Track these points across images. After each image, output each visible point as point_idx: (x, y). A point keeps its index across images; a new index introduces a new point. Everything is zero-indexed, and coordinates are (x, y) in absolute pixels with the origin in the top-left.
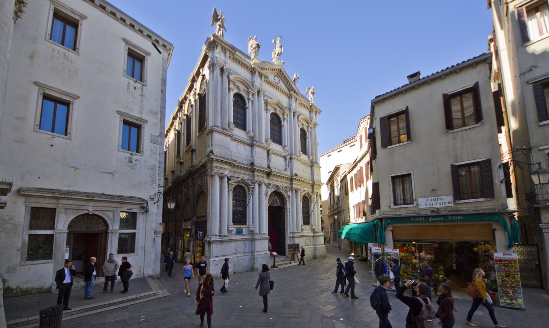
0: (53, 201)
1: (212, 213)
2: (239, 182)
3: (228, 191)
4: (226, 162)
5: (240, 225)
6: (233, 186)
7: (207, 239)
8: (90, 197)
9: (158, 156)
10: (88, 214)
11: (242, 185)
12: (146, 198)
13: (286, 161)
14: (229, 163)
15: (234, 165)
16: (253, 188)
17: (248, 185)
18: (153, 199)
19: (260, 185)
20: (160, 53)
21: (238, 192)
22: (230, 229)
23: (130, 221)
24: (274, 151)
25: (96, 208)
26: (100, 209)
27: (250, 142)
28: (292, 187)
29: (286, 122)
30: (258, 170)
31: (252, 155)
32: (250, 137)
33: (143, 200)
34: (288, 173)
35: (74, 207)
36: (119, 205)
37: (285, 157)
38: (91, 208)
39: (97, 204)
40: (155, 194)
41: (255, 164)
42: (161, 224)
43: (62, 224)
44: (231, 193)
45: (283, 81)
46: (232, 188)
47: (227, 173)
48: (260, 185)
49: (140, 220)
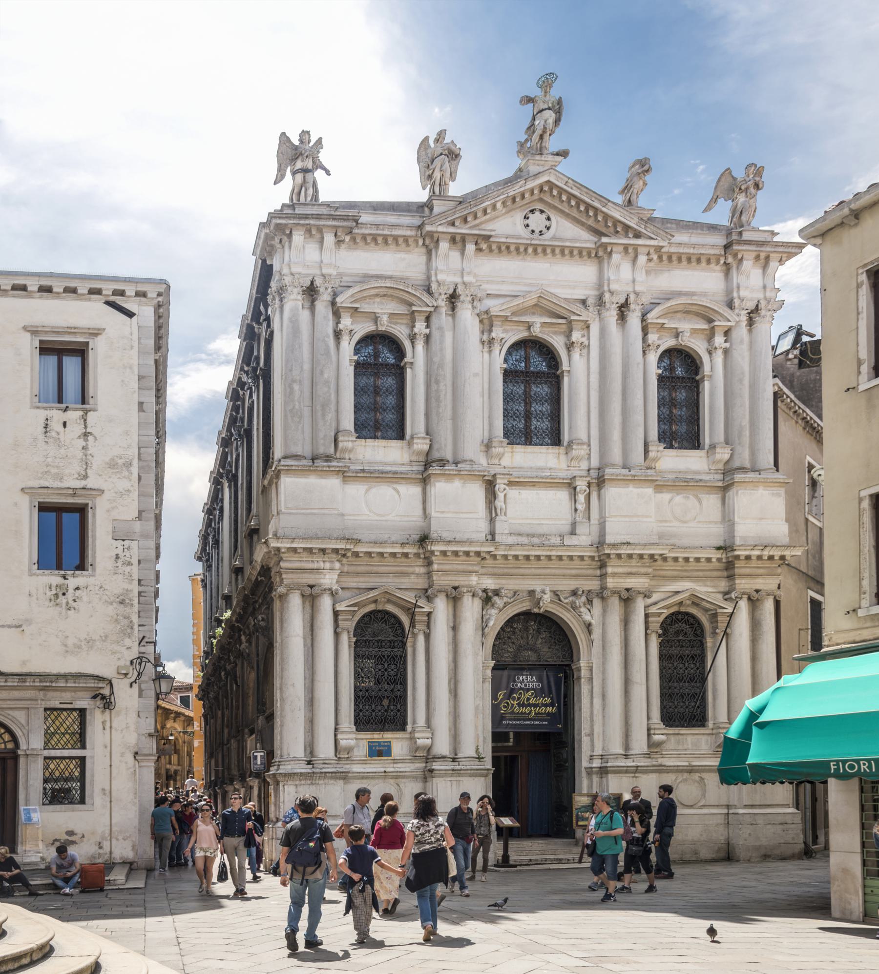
1: (282, 699)
2: (376, 601)
3: (337, 634)
4: (323, 551)
5: (382, 730)
6: (357, 618)
7: (273, 770)
9: (135, 568)
11: (390, 608)
14: (336, 551)
15: (356, 555)
28: (603, 588)
29: (576, 354)
30: (444, 553)
31: (424, 509)
32: (419, 453)
34: (585, 538)
37: (571, 486)
40: (132, 662)
41: (434, 535)
42: (150, 735)
46: (349, 625)
47: (329, 580)
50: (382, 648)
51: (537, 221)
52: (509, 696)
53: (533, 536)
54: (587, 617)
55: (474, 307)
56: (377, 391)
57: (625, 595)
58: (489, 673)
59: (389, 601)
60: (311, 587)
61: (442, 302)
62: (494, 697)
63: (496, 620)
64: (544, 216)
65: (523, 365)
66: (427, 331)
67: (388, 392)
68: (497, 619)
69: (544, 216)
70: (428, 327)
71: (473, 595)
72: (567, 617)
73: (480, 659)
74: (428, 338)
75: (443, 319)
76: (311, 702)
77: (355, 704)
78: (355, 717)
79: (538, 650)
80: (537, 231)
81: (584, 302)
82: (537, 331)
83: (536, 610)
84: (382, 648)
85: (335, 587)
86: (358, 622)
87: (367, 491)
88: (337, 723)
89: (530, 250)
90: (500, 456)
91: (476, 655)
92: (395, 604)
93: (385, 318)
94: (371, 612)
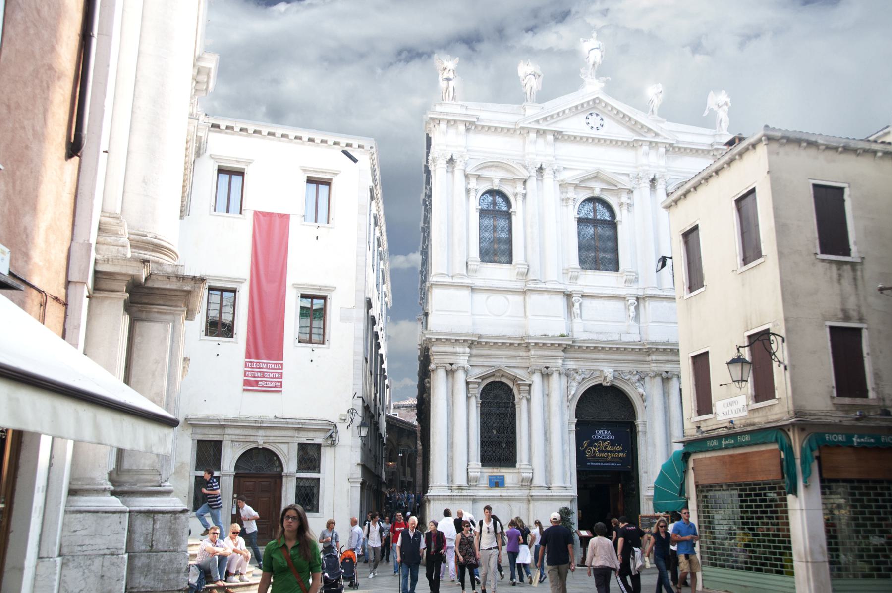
0: (219, 431)
2: (492, 375)
3: (468, 398)
6: (482, 386)
8: (259, 426)
10: (257, 448)
11: (504, 380)
12: (335, 419)
13: (627, 308)
16: (530, 385)
17: (515, 379)
18: (345, 420)
19: (546, 375)
20: (355, 161)
21: (495, 397)
22: (471, 474)
23: (309, 457)
24: (587, 291)
25: (266, 439)
26: (271, 439)
27: (519, 285)
32: (521, 274)
33: (330, 423)
35: (242, 438)
36: (295, 434)
38: (260, 440)
39: (268, 433)
43: (229, 458)
44: (473, 401)
45: (614, 119)
46: (477, 391)
48: (546, 375)
49: (327, 457)
50: (498, 408)
51: (594, 121)
52: (590, 445)
53: (601, 333)
54: (641, 390)
55: (555, 177)
56: (495, 229)
57: (664, 375)
58: (573, 427)
59: (502, 376)
60: (452, 365)
61: (533, 173)
62: (579, 443)
63: (577, 390)
64: (599, 118)
65: (592, 214)
66: (524, 192)
67: (502, 230)
68: (577, 390)
69: (599, 118)
70: (525, 189)
71: (560, 374)
72: (627, 389)
73: (567, 418)
74: (525, 196)
75: (532, 184)
76: (451, 445)
77: (481, 447)
78: (482, 456)
79: (606, 415)
80: (595, 127)
81: (628, 175)
82: (597, 193)
83: (604, 384)
84: (498, 408)
85: (467, 366)
86: (483, 389)
87: (488, 298)
88: (468, 460)
89: (590, 140)
90: (576, 278)
91: (562, 414)
92: (507, 378)
93: (496, 182)
94: (492, 382)
